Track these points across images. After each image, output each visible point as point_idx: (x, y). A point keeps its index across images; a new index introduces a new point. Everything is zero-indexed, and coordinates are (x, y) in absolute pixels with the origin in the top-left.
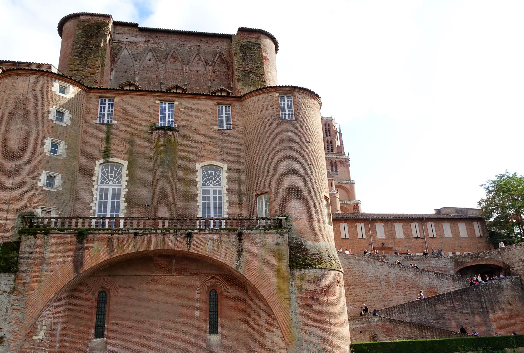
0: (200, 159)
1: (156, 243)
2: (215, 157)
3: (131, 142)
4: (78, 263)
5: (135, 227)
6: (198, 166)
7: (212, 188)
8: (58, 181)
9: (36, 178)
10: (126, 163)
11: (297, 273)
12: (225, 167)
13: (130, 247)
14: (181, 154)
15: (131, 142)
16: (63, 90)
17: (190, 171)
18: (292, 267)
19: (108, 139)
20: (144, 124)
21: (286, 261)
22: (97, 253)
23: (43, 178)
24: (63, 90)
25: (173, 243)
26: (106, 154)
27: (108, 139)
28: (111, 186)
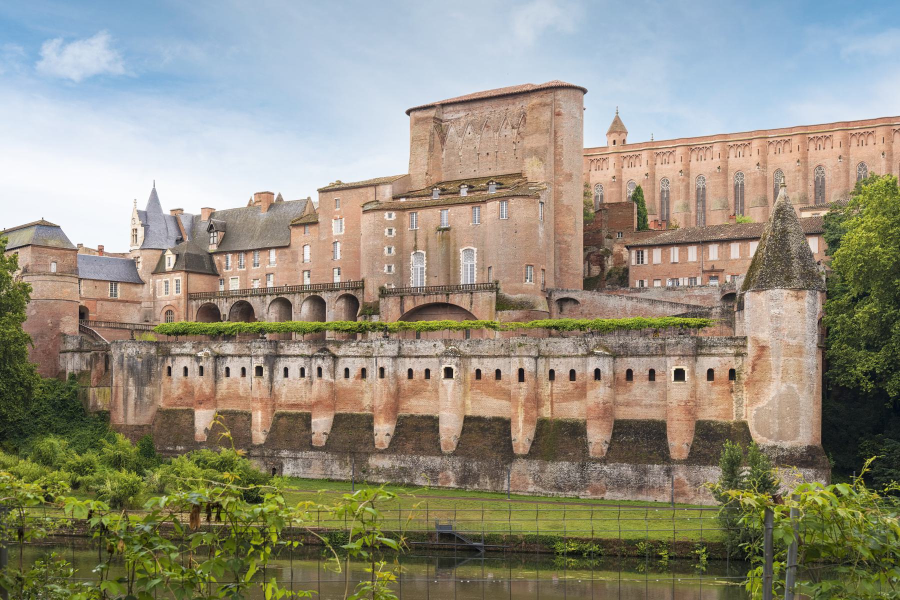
0: (462, 246)
1: (433, 299)
2: (469, 243)
3: (427, 239)
4: (402, 310)
5: (428, 292)
6: (461, 250)
7: (469, 263)
8: (393, 268)
9: (383, 268)
10: (425, 253)
11: (499, 313)
12: (475, 249)
13: (422, 301)
14: (452, 244)
15: (427, 239)
16: (390, 216)
17: (456, 254)
18: (497, 310)
19: (416, 239)
20: (432, 228)
21: (494, 306)
22: (409, 305)
23: (386, 268)
24: (390, 216)
25: (441, 299)
26: (415, 248)
27: (416, 239)
28: (419, 266)
